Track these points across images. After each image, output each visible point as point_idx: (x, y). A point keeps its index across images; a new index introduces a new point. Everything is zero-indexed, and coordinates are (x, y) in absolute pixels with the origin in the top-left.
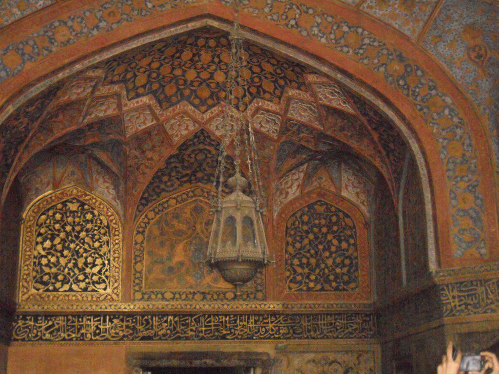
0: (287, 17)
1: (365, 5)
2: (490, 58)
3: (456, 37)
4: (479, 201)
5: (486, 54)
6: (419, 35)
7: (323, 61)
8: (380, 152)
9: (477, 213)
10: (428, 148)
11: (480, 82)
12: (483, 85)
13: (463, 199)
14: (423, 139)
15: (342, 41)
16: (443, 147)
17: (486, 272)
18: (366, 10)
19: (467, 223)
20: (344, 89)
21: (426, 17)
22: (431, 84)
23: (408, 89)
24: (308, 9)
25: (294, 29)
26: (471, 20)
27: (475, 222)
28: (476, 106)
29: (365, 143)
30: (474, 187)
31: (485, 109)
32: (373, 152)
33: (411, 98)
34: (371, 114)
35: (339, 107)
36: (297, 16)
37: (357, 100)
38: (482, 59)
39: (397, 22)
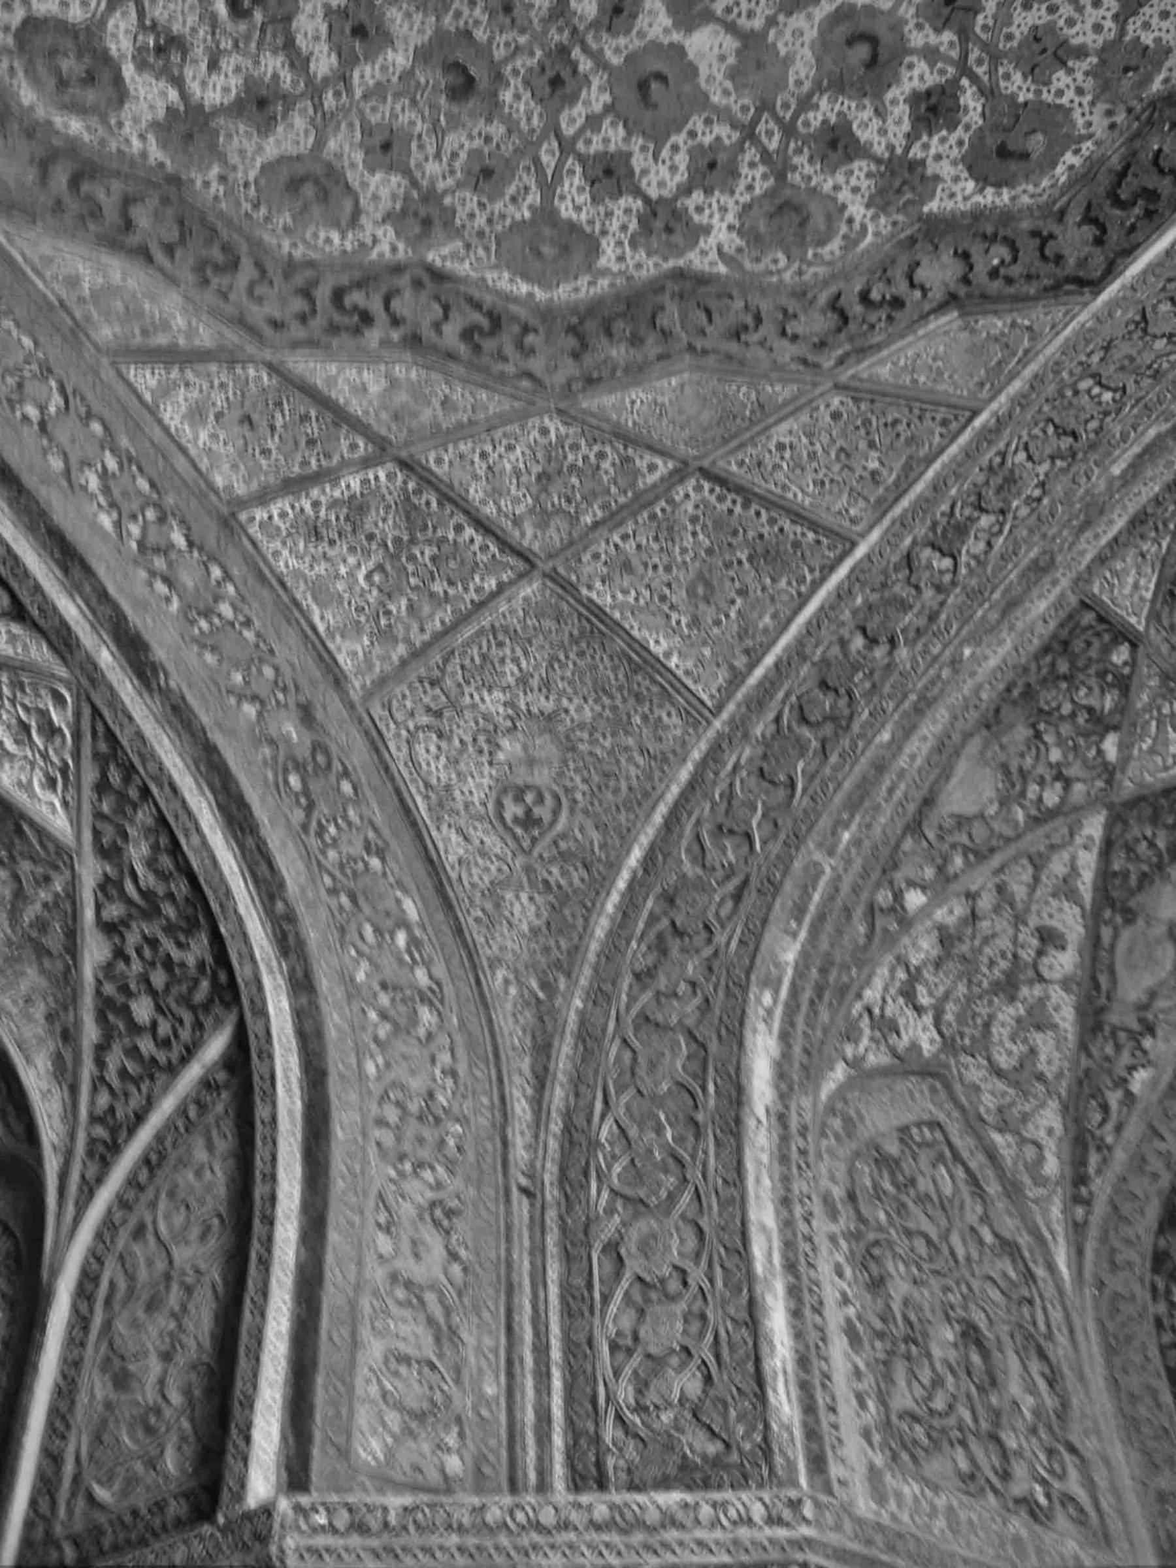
0: (20, 386)
1: (260, 514)
2: (564, 836)
3: (481, 739)
4: (456, 1269)
5: (553, 822)
6: (382, 682)
7: (76, 572)
8: (68, 1036)
9: (448, 1312)
10: (334, 1021)
11: (509, 896)
12: (517, 909)
13: (414, 1243)
14: (324, 983)
15: (159, 563)
16: (376, 1039)
17: (536, 1537)
18: (253, 530)
19: (412, 1334)
20: (96, 712)
21: (426, 637)
22: (371, 835)
23: (310, 808)
24: (89, 415)
25: (26, 429)
26: (549, 706)
27: (438, 1339)
28: (485, 963)
29: (24, 986)
30: (450, 1213)
31: (507, 982)
32: (40, 1031)
33: (314, 842)
34: (137, 852)
35: (20, 798)
36: (52, 409)
37: (115, 777)
38: (536, 833)
39: (329, 616)
